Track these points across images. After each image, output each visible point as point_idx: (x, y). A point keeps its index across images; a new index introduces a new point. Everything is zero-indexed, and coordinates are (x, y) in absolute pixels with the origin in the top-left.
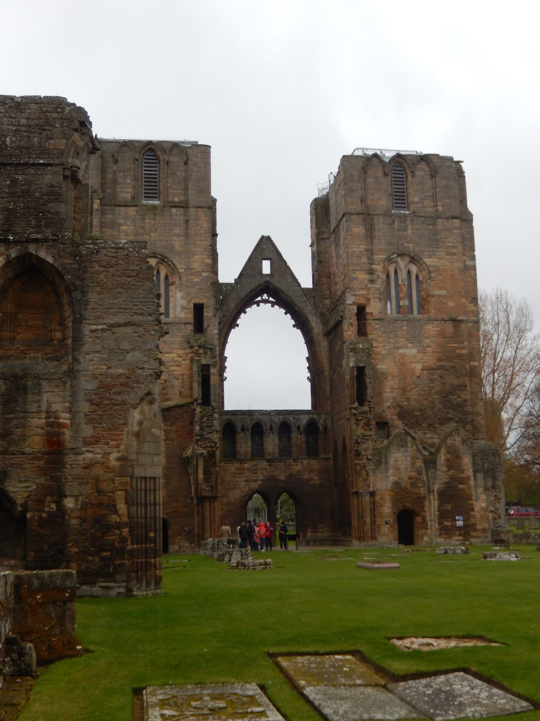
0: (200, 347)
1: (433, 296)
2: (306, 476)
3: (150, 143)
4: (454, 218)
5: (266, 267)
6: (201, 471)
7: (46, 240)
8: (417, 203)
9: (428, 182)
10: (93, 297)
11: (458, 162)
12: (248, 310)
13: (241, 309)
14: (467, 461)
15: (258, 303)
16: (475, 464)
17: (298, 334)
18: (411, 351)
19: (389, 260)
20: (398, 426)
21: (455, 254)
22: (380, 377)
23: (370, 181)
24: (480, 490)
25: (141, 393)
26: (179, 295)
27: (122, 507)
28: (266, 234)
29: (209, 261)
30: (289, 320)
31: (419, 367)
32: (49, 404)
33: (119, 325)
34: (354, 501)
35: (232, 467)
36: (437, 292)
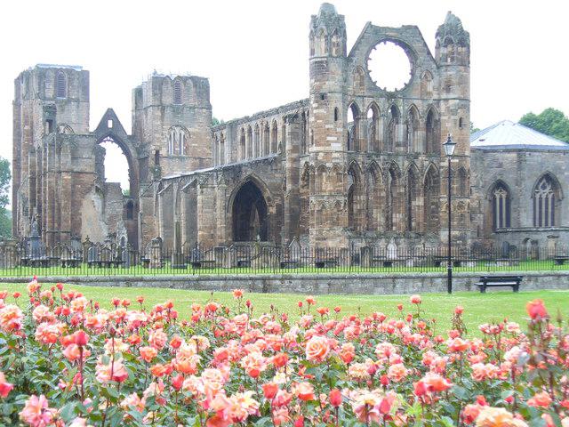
5: (110, 124)
17: (124, 157)
30: (120, 150)
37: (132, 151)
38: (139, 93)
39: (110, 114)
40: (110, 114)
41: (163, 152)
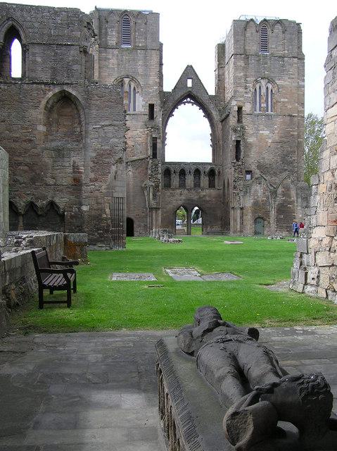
0: (152, 128)
1: (280, 102)
2: (208, 199)
3: (126, 11)
4: (295, 58)
6: (151, 194)
7: (72, 84)
8: (274, 48)
9: (281, 35)
10: (94, 112)
11: (298, 24)
12: (179, 107)
13: (175, 107)
14: (293, 193)
15: (184, 103)
16: (297, 194)
17: (206, 121)
18: (266, 133)
19: (256, 81)
20: (257, 173)
21: (293, 78)
22: (248, 146)
23: (248, 34)
24: (299, 208)
25: (117, 158)
26: (141, 99)
27: (108, 210)
28: (190, 64)
29: (158, 80)
30: (201, 113)
31: (270, 141)
32: (74, 162)
33: (106, 126)
34: (232, 212)
35: (168, 193)
36: (282, 100)
37: (215, 113)
38: (221, 49)
39: (189, 72)
40: (189, 72)
41: (247, 108)
